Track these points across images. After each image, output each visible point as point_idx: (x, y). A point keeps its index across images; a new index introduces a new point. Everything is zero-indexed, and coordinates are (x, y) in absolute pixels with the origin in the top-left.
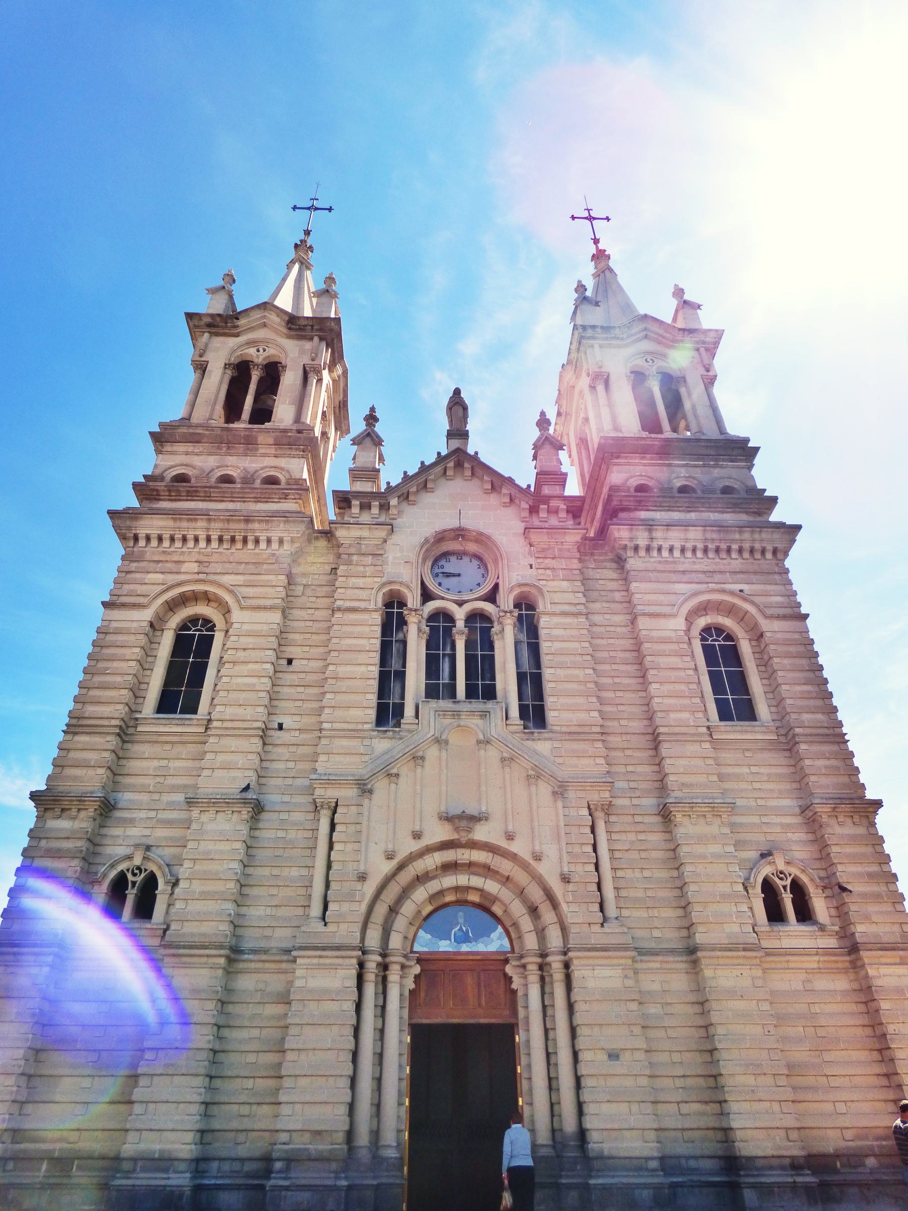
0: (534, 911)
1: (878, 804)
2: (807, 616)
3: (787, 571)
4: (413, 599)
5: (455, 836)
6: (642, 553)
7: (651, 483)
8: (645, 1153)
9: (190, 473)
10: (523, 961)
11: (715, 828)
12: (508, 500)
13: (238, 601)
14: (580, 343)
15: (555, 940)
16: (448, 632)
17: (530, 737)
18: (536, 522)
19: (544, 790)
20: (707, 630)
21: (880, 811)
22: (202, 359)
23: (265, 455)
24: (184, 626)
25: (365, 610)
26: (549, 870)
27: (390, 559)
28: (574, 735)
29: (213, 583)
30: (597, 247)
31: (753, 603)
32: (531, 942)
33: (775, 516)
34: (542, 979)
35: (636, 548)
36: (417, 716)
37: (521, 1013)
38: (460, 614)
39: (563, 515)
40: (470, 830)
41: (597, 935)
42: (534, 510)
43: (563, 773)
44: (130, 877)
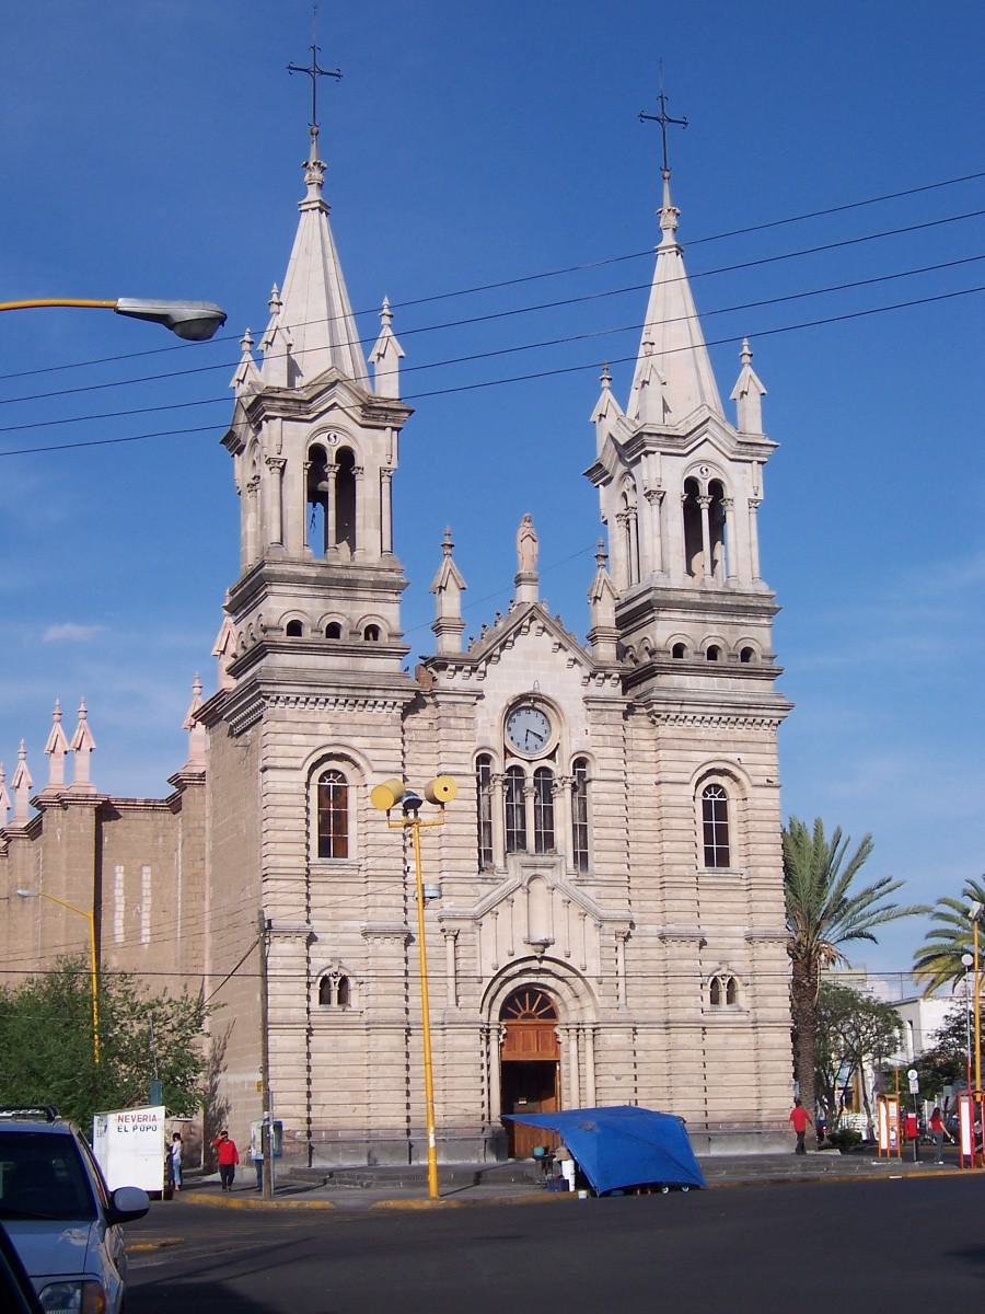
16: (521, 784)
17: (581, 883)
19: (590, 921)
24: (321, 779)
27: (479, 723)
38: (530, 771)
43: (604, 913)
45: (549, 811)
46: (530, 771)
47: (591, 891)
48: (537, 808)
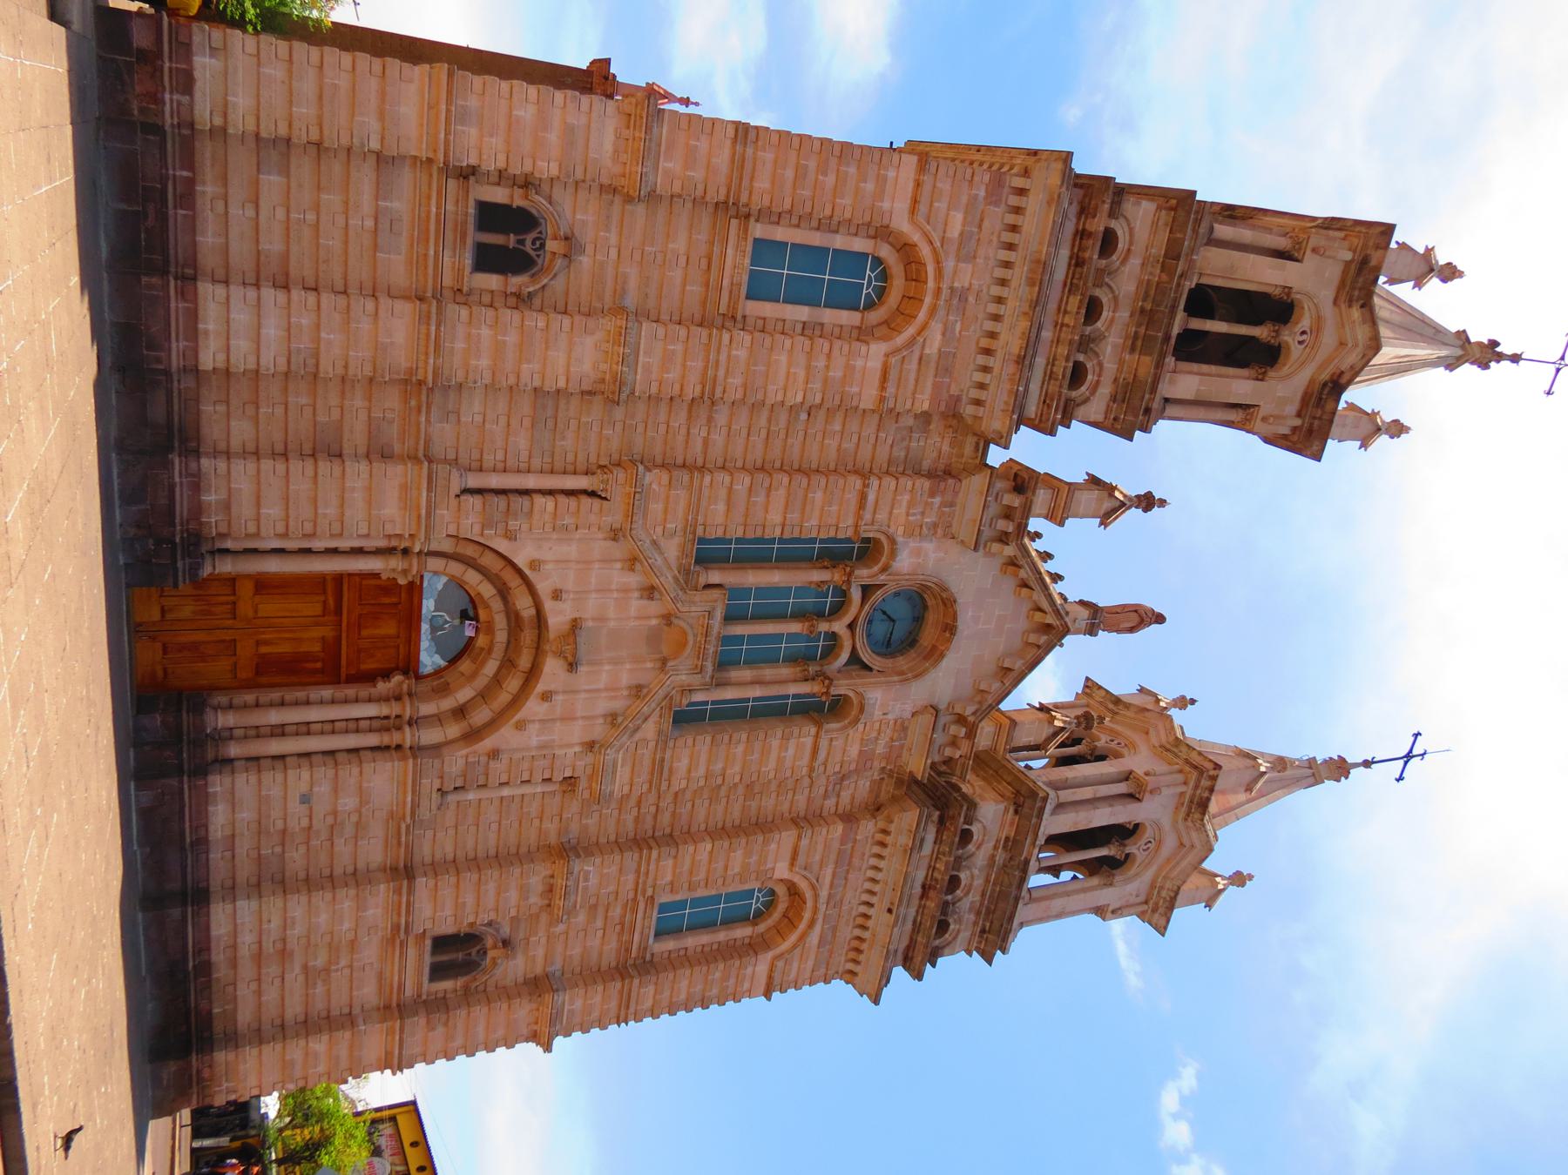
0: (460, 712)
1: (548, 1048)
2: (769, 999)
3: (827, 981)
4: (864, 574)
5: (552, 635)
6: (879, 836)
7: (971, 847)
8: (211, 828)
9: (1114, 257)
10: (406, 699)
11: (535, 900)
12: (982, 687)
13: (898, 350)
14: (1196, 767)
15: (429, 736)
18: (943, 720)
19: (599, 731)
20: (772, 892)
21: (540, 1049)
22: (1308, 252)
23: (1121, 362)
24: (878, 261)
25: (859, 517)
26: (505, 737)
28: (659, 769)
29: (933, 311)
30: (1356, 765)
31: (795, 947)
32: (427, 709)
33: (899, 973)
34: (388, 748)
35: (885, 832)
36: (708, 586)
37: (350, 691)
39: (948, 752)
40: (560, 654)
41: (429, 784)
42: (961, 720)
44: (533, 235)
45: (772, 660)
46: (839, 627)
47: (649, 730)
48: (777, 638)
